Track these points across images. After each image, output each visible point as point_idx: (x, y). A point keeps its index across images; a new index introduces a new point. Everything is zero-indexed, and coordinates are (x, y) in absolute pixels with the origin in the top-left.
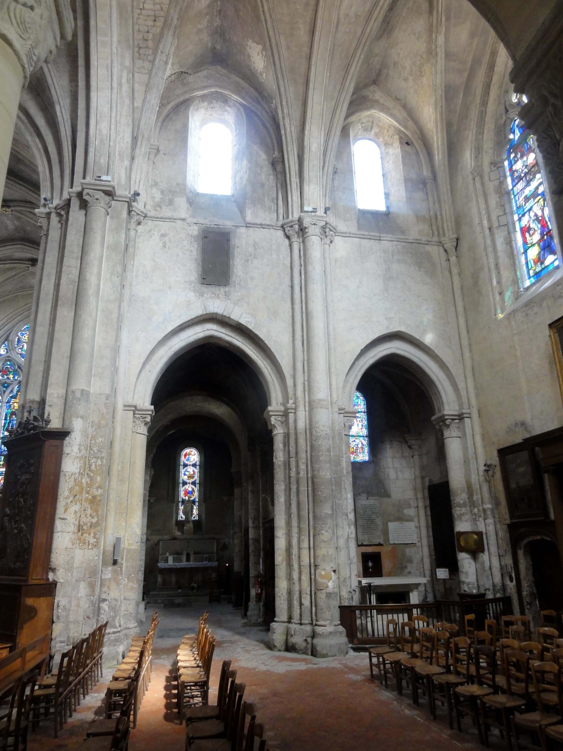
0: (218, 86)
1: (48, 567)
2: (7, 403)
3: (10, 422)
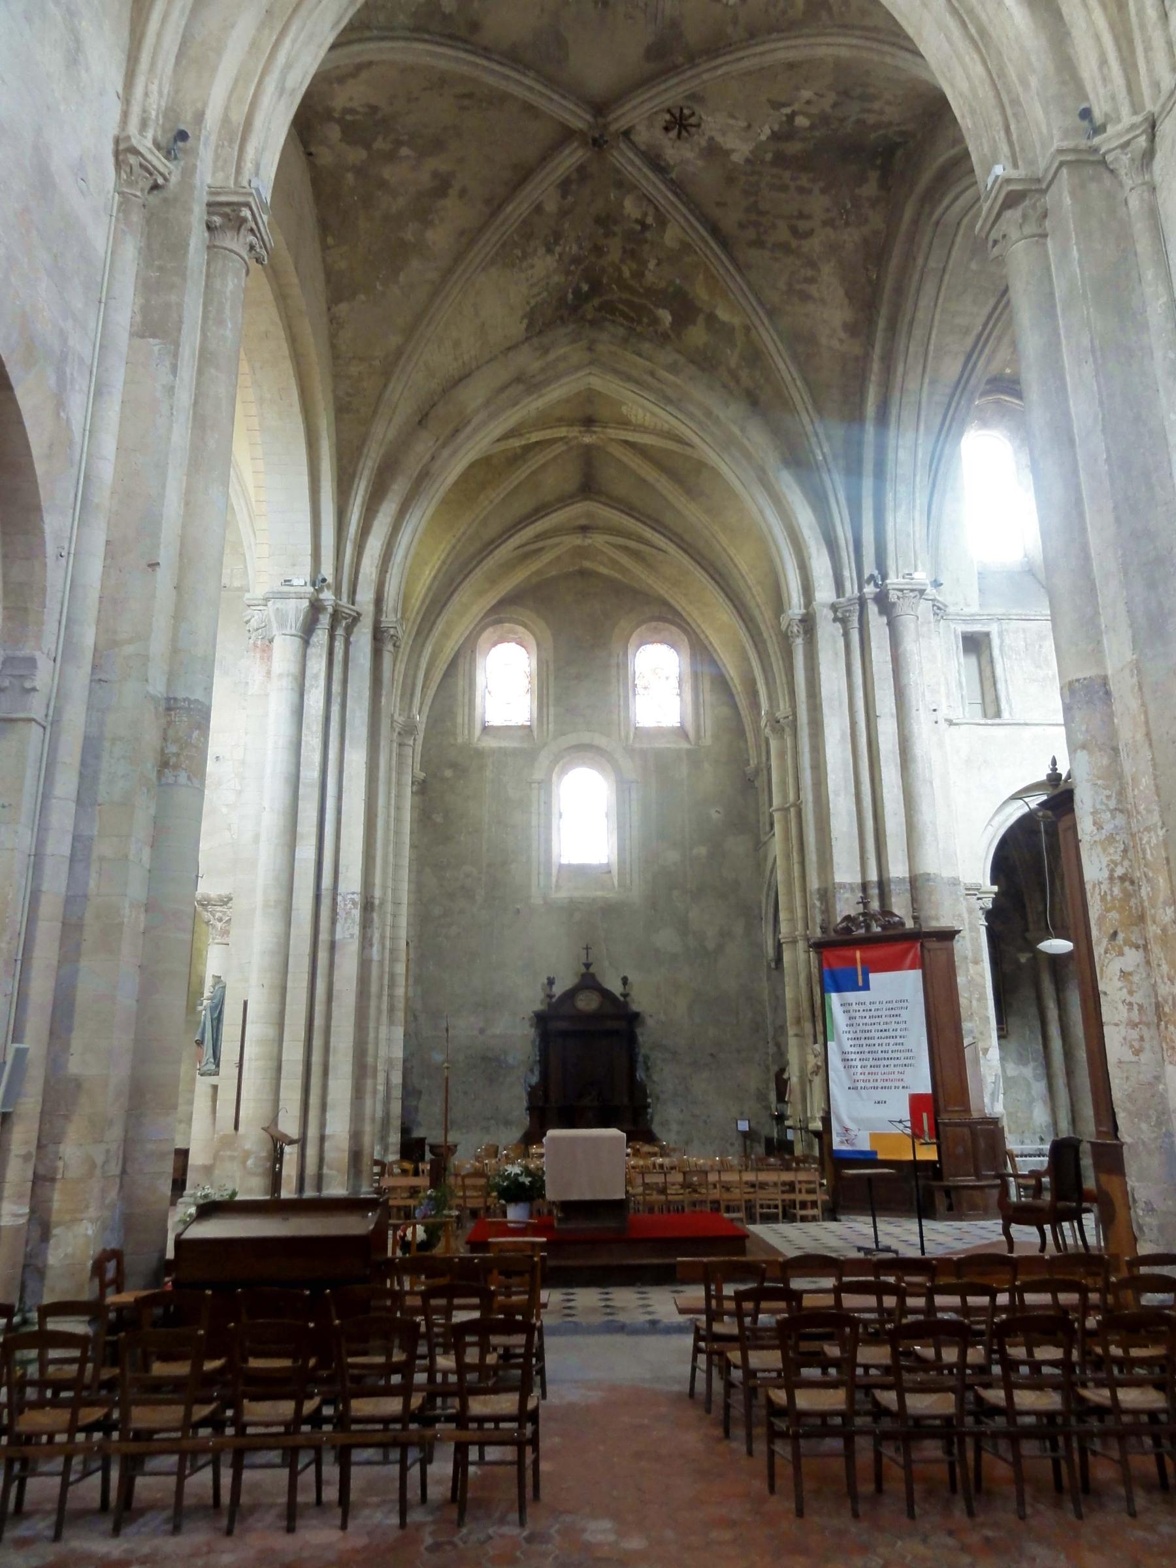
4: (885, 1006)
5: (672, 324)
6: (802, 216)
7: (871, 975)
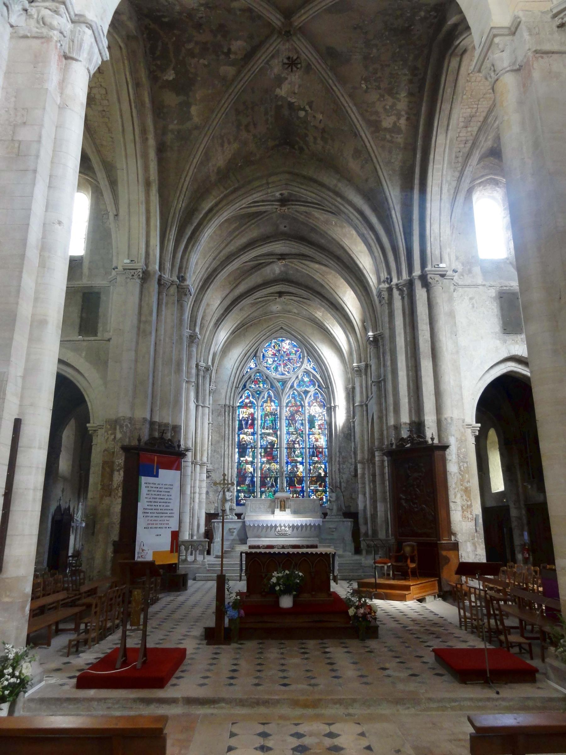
0: (491, 174)
1: (451, 533)
2: (261, 406)
3: (265, 422)
4: (164, 486)
5: (167, 80)
6: (255, 125)
7: (161, 471)
